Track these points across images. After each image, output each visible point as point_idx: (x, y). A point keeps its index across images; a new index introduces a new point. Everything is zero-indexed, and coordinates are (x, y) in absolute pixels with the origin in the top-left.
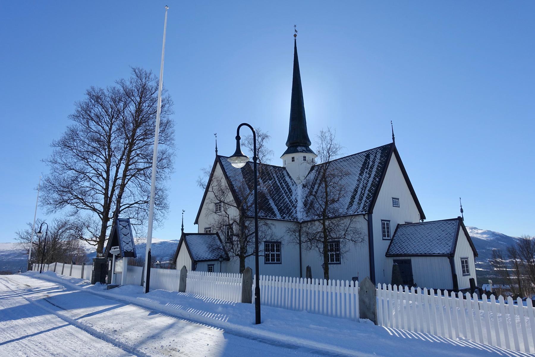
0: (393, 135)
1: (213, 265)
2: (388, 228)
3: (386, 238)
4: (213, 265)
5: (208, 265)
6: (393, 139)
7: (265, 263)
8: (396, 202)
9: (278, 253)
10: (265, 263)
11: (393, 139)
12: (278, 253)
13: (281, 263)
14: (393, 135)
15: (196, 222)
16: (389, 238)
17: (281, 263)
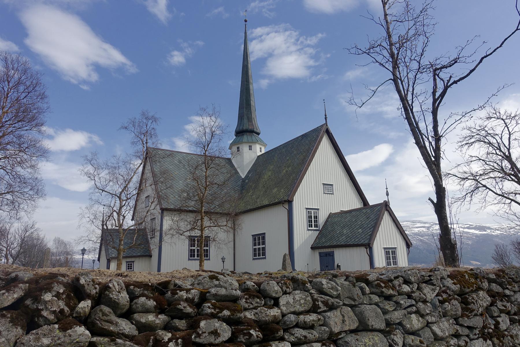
0: (326, 116)
1: (133, 262)
2: (316, 217)
3: (313, 228)
4: (133, 262)
5: (127, 262)
6: (326, 118)
7: (189, 259)
8: (328, 188)
9: (193, 248)
10: (189, 259)
11: (326, 118)
12: (193, 248)
13: (209, 259)
14: (326, 116)
15: (132, 220)
16: (318, 229)
17: (209, 259)
